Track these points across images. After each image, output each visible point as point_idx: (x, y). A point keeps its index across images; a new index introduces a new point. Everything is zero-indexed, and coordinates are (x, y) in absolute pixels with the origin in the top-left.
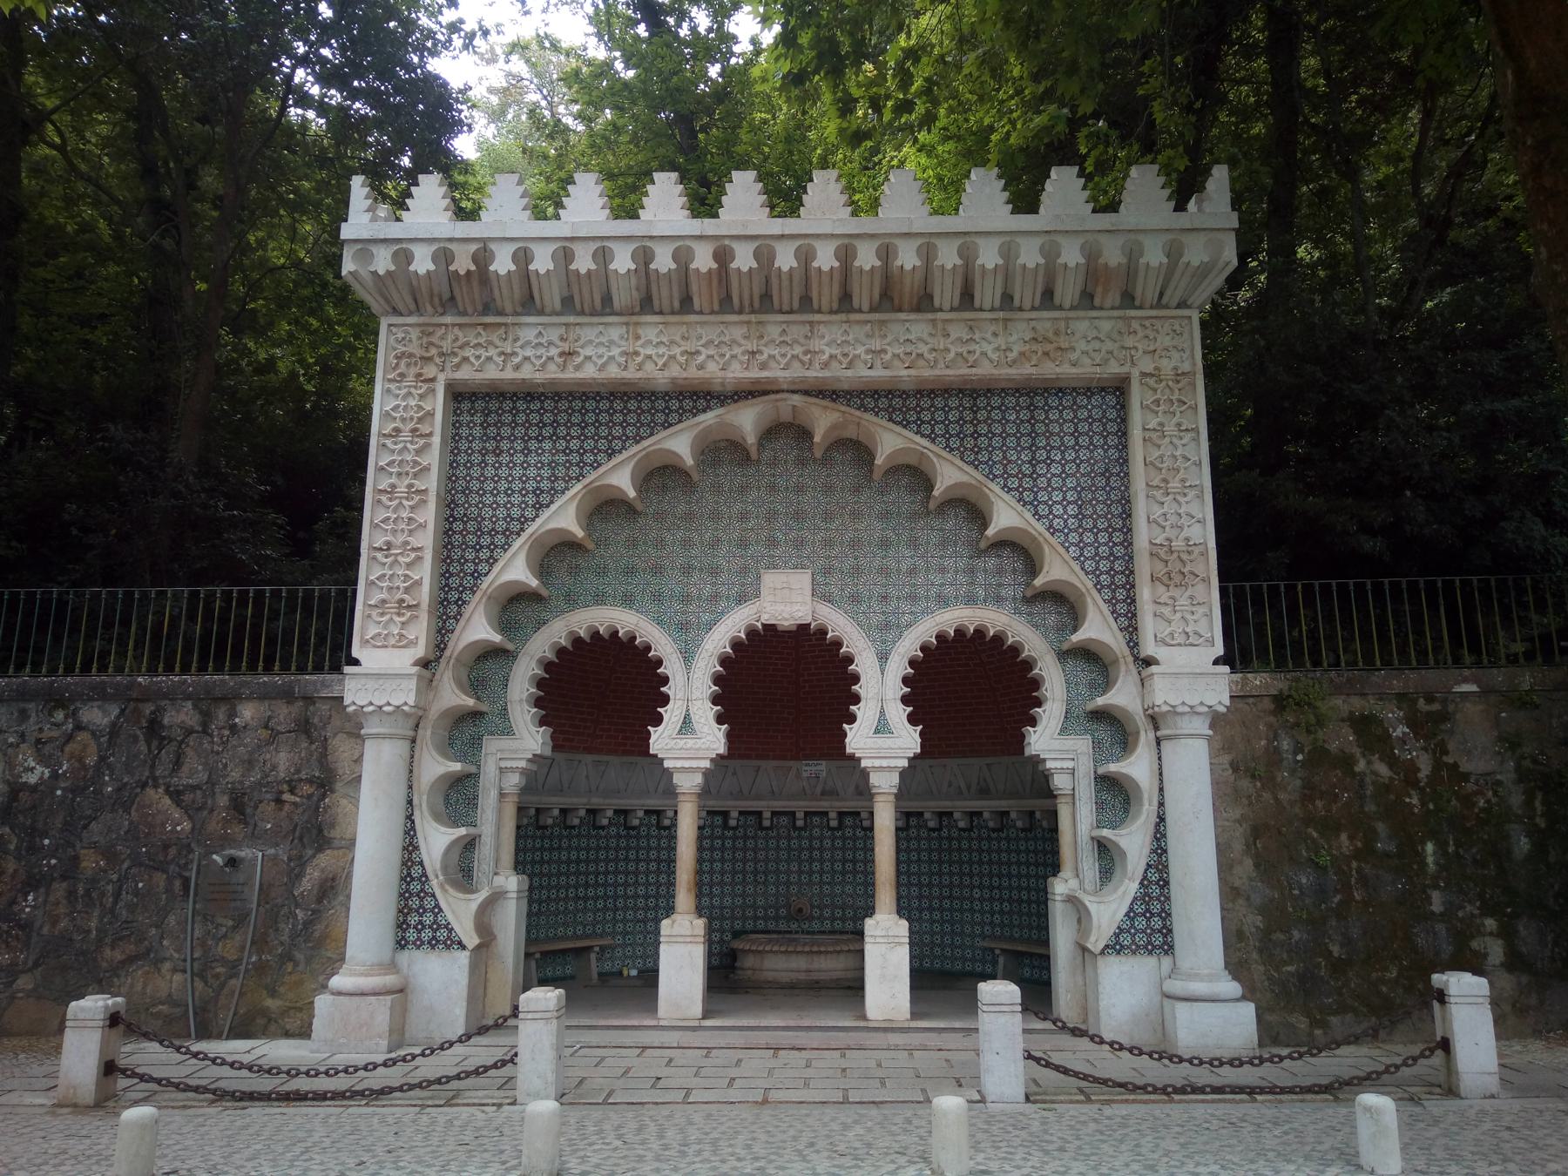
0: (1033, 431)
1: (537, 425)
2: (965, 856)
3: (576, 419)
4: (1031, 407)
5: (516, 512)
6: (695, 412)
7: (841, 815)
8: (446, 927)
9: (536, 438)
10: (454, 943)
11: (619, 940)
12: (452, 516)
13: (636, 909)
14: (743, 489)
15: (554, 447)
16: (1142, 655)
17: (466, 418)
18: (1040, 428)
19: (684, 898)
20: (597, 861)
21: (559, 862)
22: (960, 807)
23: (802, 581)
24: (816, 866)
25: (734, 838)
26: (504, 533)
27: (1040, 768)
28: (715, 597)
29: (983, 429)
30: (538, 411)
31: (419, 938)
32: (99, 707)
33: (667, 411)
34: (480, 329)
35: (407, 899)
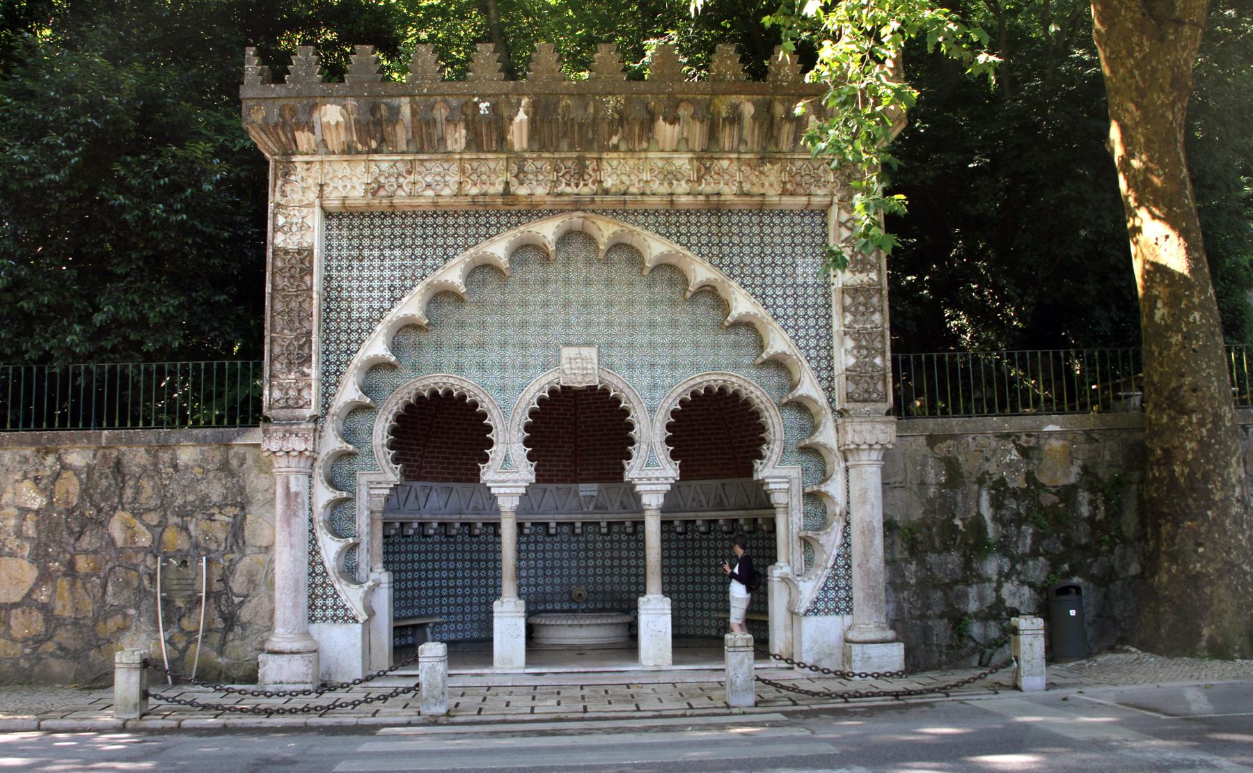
0: (762, 242)
1: (389, 237)
2: (705, 553)
3: (419, 232)
4: (761, 224)
5: (376, 305)
6: (509, 226)
7: (610, 524)
8: (343, 607)
9: (389, 247)
10: (348, 618)
11: (444, 619)
12: (328, 307)
13: (456, 596)
14: (545, 282)
15: (403, 254)
16: (838, 408)
17: (335, 232)
18: (767, 240)
19: (509, 586)
20: (426, 561)
21: (400, 562)
22: (701, 517)
23: (591, 353)
24: (591, 563)
25: (528, 543)
26: (368, 320)
27: (765, 488)
28: (525, 366)
29: (725, 240)
30: (390, 226)
31: (324, 616)
32: (78, 453)
33: (488, 225)
34: (345, 164)
35: (314, 589)
